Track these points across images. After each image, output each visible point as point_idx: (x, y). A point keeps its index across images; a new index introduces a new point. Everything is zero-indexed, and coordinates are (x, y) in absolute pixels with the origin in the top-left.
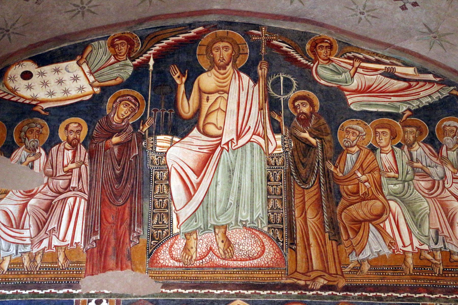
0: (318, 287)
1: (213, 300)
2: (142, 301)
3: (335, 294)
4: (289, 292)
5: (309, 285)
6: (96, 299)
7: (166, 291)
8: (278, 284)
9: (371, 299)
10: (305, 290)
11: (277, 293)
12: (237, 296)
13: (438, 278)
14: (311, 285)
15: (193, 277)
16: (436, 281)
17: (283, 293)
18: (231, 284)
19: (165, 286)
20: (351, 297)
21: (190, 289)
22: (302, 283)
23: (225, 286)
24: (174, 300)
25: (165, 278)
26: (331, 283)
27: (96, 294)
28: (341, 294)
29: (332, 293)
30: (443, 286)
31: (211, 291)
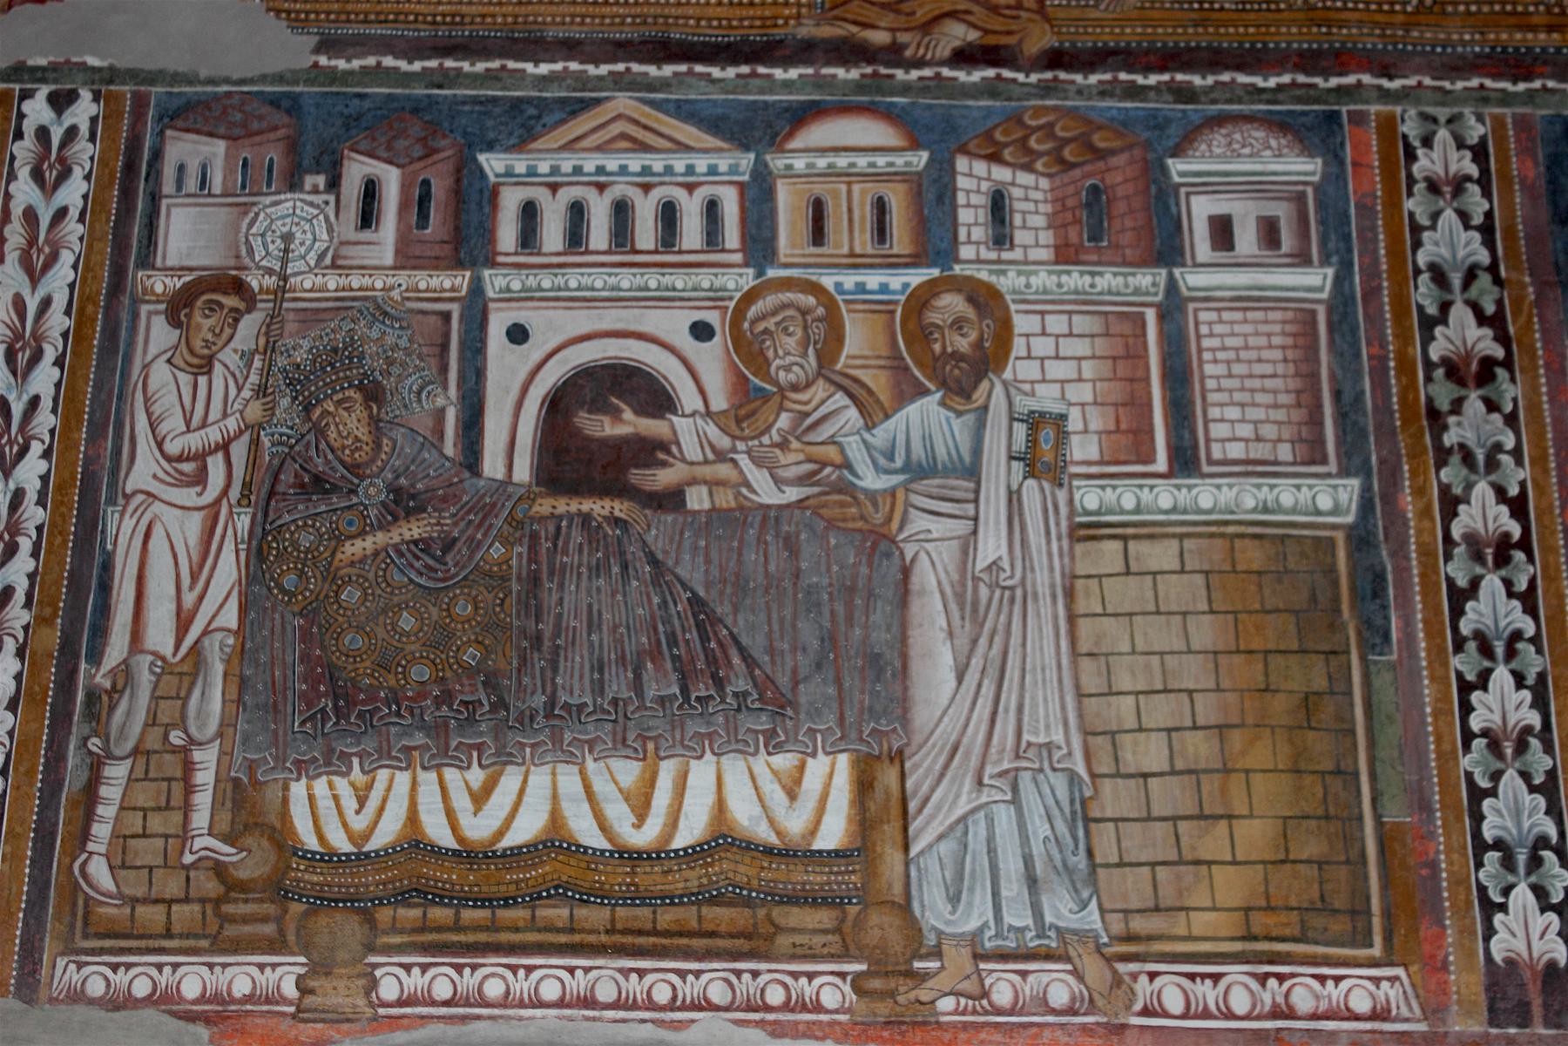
0: (944, 51)
1: (520, 100)
2: (237, 97)
3: (1006, 80)
4: (825, 71)
5: (905, 46)
6: (53, 87)
7: (333, 63)
8: (781, 41)
9: (1152, 94)
10: (888, 65)
11: (778, 73)
12: (616, 83)
13: (1413, 19)
14: (913, 46)
15: (444, 15)
16: (1407, 31)
17: (801, 76)
18: (593, 42)
19: (327, 45)
20: (1073, 88)
21: (429, 58)
22: (880, 37)
23: (570, 48)
24: (361, 96)
25: (332, 17)
26: (992, 40)
27: (54, 67)
28: (1034, 78)
29: (999, 77)
30: (1434, 47)
31: (511, 65)
